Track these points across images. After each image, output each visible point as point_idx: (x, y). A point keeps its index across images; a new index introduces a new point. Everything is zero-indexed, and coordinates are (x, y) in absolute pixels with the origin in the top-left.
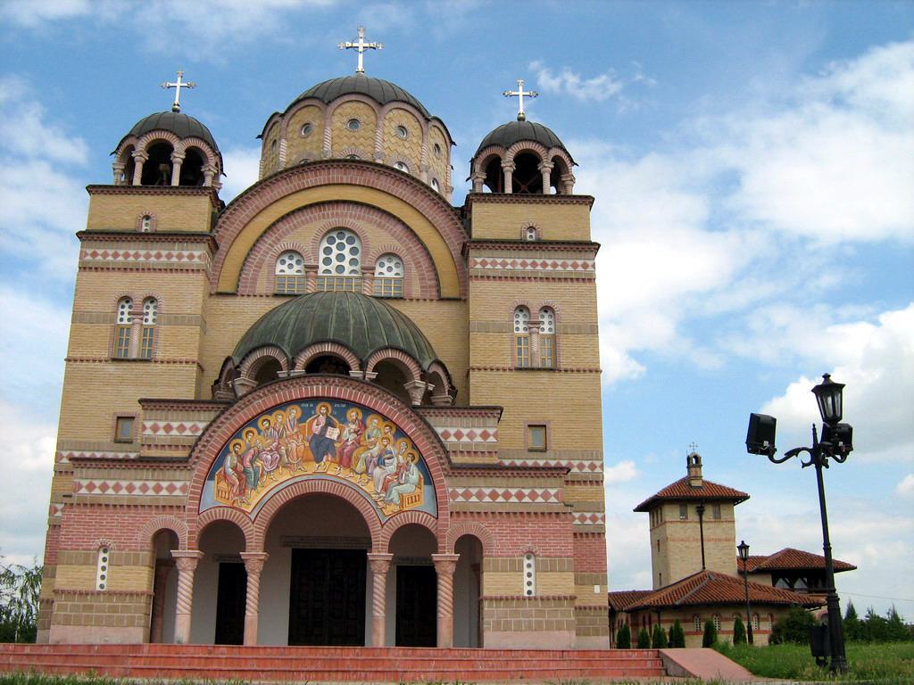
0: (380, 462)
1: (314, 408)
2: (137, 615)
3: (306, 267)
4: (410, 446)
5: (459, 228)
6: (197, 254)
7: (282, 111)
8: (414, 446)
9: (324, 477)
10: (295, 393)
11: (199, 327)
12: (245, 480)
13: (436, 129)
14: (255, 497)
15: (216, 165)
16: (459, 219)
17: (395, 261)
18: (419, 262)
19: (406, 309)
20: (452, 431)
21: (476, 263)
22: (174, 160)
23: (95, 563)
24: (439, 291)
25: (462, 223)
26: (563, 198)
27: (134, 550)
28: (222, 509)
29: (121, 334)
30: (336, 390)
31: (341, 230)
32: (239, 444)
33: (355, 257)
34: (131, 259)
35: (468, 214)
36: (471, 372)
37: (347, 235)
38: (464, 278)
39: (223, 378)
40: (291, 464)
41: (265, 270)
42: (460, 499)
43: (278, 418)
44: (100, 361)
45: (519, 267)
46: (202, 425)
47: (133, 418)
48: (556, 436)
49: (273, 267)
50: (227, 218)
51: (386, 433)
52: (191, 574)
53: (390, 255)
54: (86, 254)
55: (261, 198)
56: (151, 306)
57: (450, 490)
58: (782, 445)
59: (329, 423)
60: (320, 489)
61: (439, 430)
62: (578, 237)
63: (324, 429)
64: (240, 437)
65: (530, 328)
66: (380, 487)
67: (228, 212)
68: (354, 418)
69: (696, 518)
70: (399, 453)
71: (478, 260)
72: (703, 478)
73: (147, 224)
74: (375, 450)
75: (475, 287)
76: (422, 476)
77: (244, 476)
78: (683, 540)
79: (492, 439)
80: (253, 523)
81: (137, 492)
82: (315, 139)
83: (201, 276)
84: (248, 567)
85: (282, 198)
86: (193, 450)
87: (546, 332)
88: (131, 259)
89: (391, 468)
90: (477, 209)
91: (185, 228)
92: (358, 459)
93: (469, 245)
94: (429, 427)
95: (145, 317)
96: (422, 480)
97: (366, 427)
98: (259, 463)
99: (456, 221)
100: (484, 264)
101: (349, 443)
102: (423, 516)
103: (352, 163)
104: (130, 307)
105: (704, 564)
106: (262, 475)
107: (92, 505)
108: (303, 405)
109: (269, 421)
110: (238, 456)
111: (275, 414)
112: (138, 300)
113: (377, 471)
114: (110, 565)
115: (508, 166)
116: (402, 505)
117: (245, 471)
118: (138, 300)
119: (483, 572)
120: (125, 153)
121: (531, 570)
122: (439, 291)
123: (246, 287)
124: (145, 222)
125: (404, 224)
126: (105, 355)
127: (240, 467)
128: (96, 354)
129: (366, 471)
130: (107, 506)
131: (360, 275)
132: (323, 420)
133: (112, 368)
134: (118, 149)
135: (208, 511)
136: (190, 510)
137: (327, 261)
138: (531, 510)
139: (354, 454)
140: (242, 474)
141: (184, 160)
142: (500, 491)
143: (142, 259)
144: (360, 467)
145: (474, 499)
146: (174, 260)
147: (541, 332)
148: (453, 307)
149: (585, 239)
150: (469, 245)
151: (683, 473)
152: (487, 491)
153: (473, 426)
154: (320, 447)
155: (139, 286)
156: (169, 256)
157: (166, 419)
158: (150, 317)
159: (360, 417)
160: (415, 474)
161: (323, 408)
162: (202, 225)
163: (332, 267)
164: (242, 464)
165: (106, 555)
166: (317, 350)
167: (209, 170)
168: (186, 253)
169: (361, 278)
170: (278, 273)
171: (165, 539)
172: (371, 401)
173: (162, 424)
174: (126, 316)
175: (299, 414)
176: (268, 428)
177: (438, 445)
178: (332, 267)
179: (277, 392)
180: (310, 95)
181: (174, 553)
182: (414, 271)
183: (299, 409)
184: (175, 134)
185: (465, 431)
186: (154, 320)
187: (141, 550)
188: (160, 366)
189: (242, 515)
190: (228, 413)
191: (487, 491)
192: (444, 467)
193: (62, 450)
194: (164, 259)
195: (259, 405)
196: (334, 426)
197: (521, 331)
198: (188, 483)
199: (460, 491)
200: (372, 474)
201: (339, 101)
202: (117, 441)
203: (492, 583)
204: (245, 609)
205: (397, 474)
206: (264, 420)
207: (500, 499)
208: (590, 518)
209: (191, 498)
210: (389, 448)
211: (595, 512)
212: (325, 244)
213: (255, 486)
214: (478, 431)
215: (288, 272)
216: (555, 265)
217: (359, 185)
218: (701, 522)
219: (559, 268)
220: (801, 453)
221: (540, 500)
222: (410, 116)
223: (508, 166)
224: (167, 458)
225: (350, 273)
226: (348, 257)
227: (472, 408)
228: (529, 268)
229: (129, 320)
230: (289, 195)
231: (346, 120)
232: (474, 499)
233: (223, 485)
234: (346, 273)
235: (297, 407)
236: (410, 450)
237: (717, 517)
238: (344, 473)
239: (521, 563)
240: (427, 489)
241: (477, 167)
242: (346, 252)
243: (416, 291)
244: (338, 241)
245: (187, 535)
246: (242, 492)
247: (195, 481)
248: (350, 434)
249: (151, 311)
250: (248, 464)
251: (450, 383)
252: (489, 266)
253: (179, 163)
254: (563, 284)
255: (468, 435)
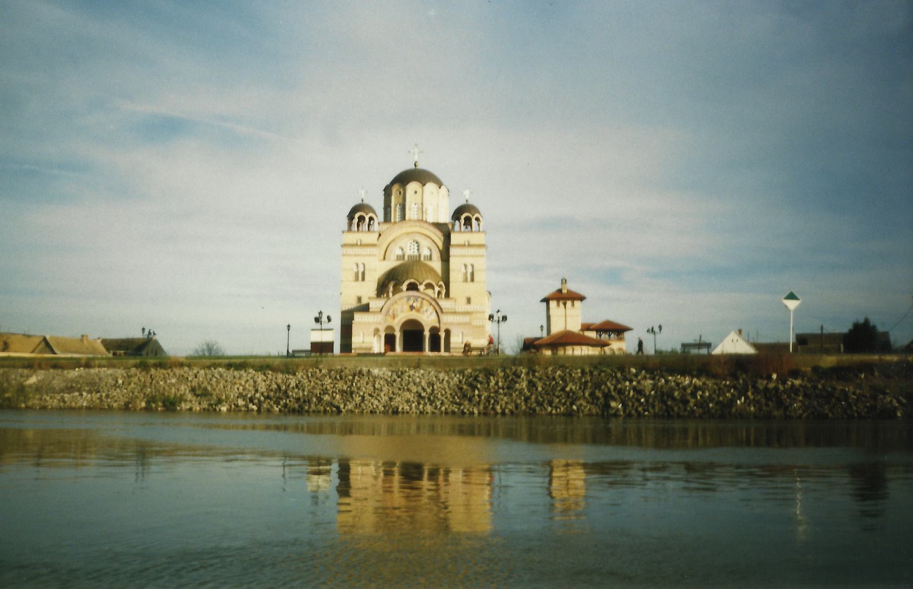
0: (426, 311)
14: (397, 320)
46: (384, 303)
59: (414, 302)
69: (563, 306)
70: (431, 309)
89: (429, 313)
132: (412, 301)
154: (412, 308)
246: (394, 318)
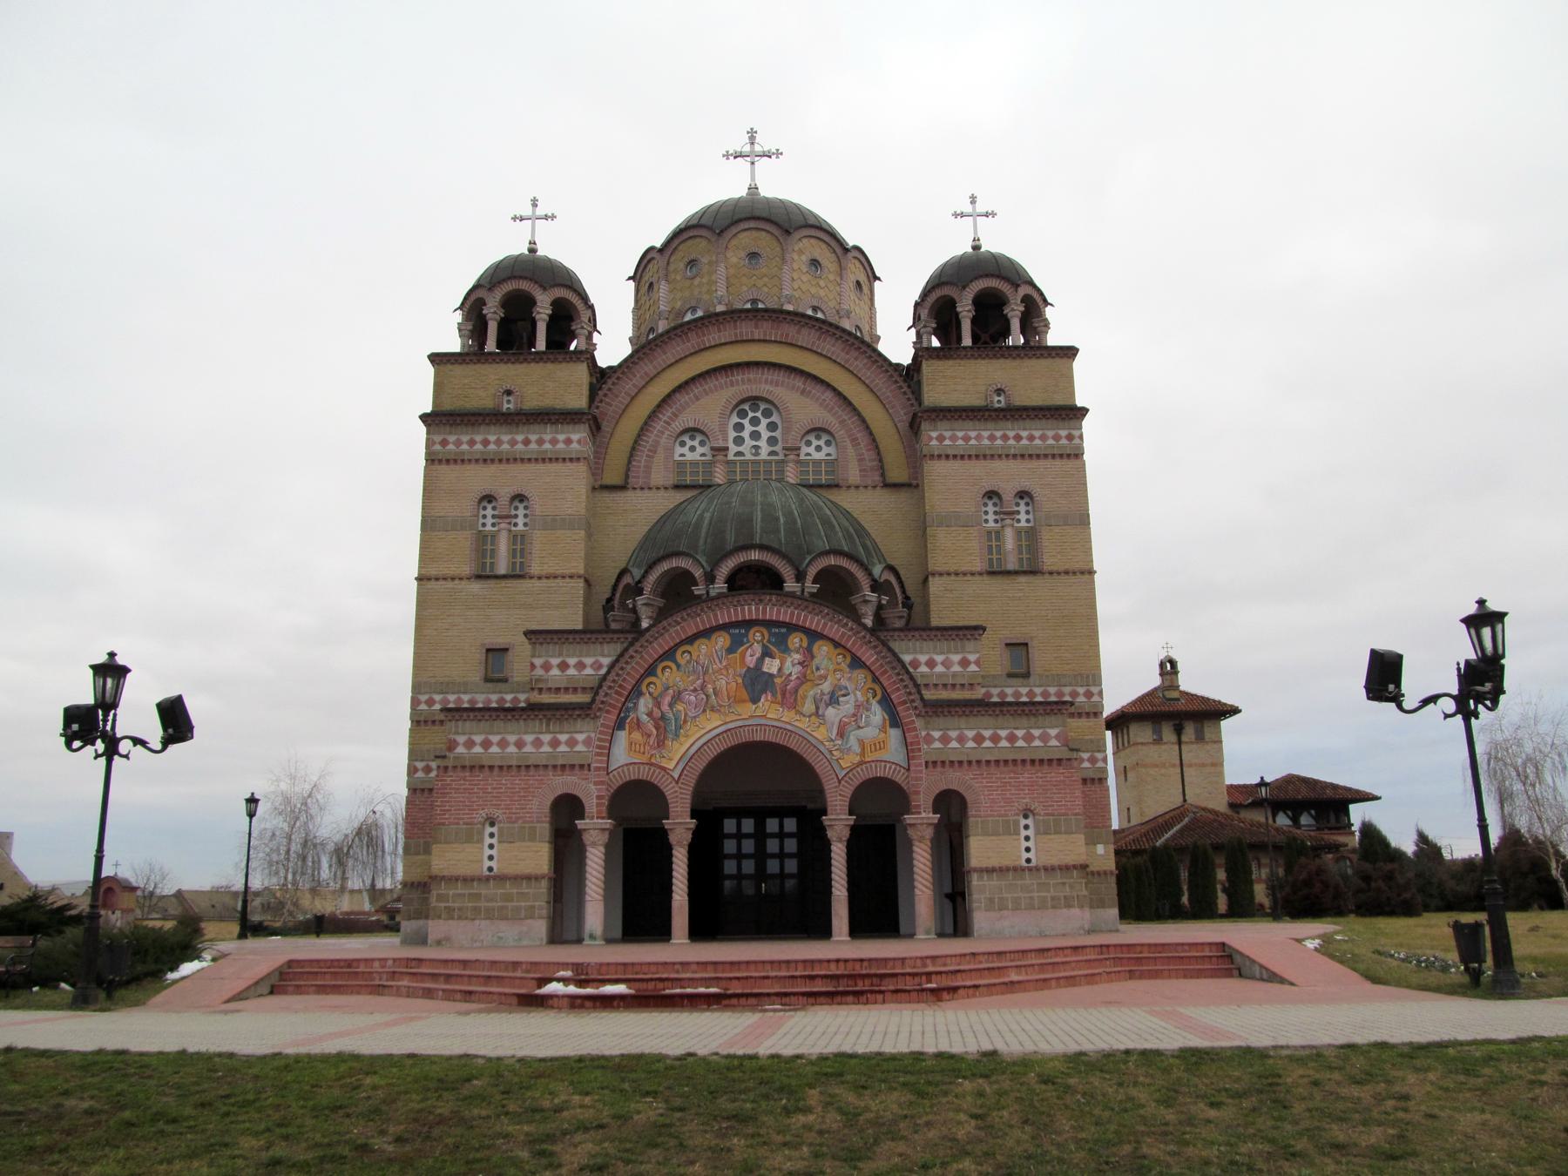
0: (833, 700)
1: (746, 635)
2: (537, 904)
3: (712, 449)
4: (870, 678)
5: (905, 393)
6: (576, 438)
7: (658, 244)
8: (876, 680)
9: (763, 721)
10: (723, 617)
11: (583, 532)
12: (664, 729)
13: (857, 262)
15: (589, 321)
16: (905, 381)
17: (825, 437)
18: (857, 439)
19: (845, 500)
20: (923, 658)
21: (931, 439)
22: (537, 317)
23: (481, 841)
24: (883, 475)
25: (909, 387)
26: (1036, 349)
27: (532, 822)
28: (636, 766)
29: (484, 542)
30: (773, 610)
31: (754, 401)
32: (654, 684)
33: (773, 434)
34: (492, 447)
35: (915, 375)
36: (930, 579)
37: (763, 406)
38: (916, 458)
39: (618, 595)
40: (721, 706)
41: (660, 455)
42: (937, 745)
43: (702, 648)
44: (461, 579)
45: (986, 442)
46: (606, 661)
47: (507, 650)
48: (1040, 659)
49: (672, 450)
50: (610, 389)
51: (839, 664)
52: (603, 849)
53: (818, 431)
54: (434, 443)
55: (651, 362)
56: (521, 506)
57: (924, 733)
58: (1413, 685)
59: (766, 653)
60: (758, 737)
61: (907, 658)
62: (1059, 400)
63: (761, 660)
64: (656, 676)
65: (1002, 520)
66: (835, 731)
67: (610, 382)
68: (797, 645)
69: (1174, 738)
70: (856, 686)
71: (935, 436)
72: (1181, 688)
73: (509, 402)
74: (826, 687)
75: (936, 472)
76: (887, 717)
77: (661, 723)
78: (1156, 766)
79: (973, 668)
80: (677, 782)
81: (528, 749)
82: (704, 280)
83: (582, 468)
84: (673, 838)
85: (677, 362)
86: (597, 693)
87: (1023, 524)
88: (492, 447)
89: (847, 706)
90: (927, 368)
91: (559, 404)
92: (804, 698)
93: (920, 416)
94: (895, 655)
95: (514, 521)
96: (888, 722)
97: (813, 657)
98: (680, 707)
99: (901, 383)
100: (941, 438)
101: (793, 677)
102: (890, 768)
103: (756, 314)
104: (494, 508)
105: (1184, 795)
106: (685, 722)
107: (472, 767)
108: (732, 631)
109: (689, 652)
110: (655, 699)
111: (697, 642)
112: (503, 500)
113: (831, 713)
114: (499, 842)
115: (965, 310)
116: (863, 754)
117: (663, 717)
118: (503, 500)
119: (967, 837)
120: (473, 307)
121: (1030, 832)
122: (883, 475)
123: (638, 477)
124: (506, 398)
125: (834, 389)
126: (466, 570)
127: (657, 713)
128: (453, 570)
129: (817, 714)
130: (491, 768)
131: (781, 457)
132: (758, 648)
133: (476, 587)
134: (463, 304)
135: (620, 770)
136: (598, 769)
137: (739, 441)
138: (1027, 756)
139: (801, 692)
140: (660, 722)
141: (551, 317)
142: (987, 733)
143: (506, 447)
144: (809, 707)
145: (954, 744)
146: (547, 446)
147: (1016, 525)
148: (902, 497)
149: (1068, 403)
150: (920, 416)
151: (1154, 681)
152: (970, 734)
153: (949, 652)
154: (757, 684)
155: (503, 481)
156: (540, 442)
157: (560, 655)
158: (520, 521)
159: (805, 644)
160: (877, 715)
161: (758, 634)
162: (579, 401)
164: (659, 708)
165: (494, 830)
166: (742, 558)
167: (582, 328)
168: (561, 437)
169: (783, 461)
170: (677, 458)
171: (567, 809)
172: (818, 624)
173: (555, 661)
174: (489, 521)
175: (728, 643)
176: (689, 662)
177: (905, 677)
179: (699, 615)
180: (695, 222)
181: (580, 824)
182: (851, 451)
183: (727, 637)
184: (536, 282)
185: (939, 658)
186: (525, 525)
187: (538, 822)
188: (536, 582)
189: (663, 773)
190: (638, 644)
191: (970, 734)
192: (914, 704)
193: (420, 693)
194: (533, 446)
195: (677, 632)
196: (772, 657)
197: (991, 524)
198: (593, 735)
199: (936, 734)
200: (823, 715)
201: (734, 230)
202: (487, 680)
203: (980, 850)
204: (671, 891)
205: (854, 715)
206: (684, 652)
207: (987, 744)
208: (1088, 760)
209: (598, 754)
210: (844, 682)
211: (1093, 751)
212: (735, 419)
213: (677, 735)
214: (956, 658)
215: (690, 456)
216: (1031, 438)
217: (775, 342)
218: (1180, 743)
219: (1037, 442)
220: (1441, 701)
221: (1037, 743)
222: (824, 246)
223: (965, 310)
224: (565, 704)
225: (769, 455)
226: (765, 434)
227: (931, 629)
228: (999, 442)
229: (493, 525)
230: (686, 357)
231: (743, 254)
232: (954, 744)
233: (637, 736)
234: (764, 455)
235: (724, 634)
236: (870, 684)
237: (1200, 738)
238: (788, 716)
239: (1017, 823)
240: (894, 734)
241: (924, 313)
242: (762, 428)
243: (854, 475)
244: (751, 415)
245: (595, 801)
246: (661, 744)
247: (601, 733)
248: (793, 665)
249: (521, 512)
250: (665, 708)
251: (904, 592)
252: (947, 442)
253: (544, 320)
254: (1042, 462)
255: (943, 663)
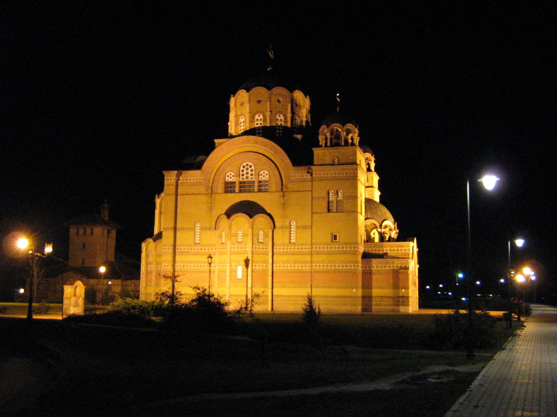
163: (244, 177)
178: (244, 177)
226: (250, 173)
234: (249, 179)
242: (249, 171)
244: (246, 167)
